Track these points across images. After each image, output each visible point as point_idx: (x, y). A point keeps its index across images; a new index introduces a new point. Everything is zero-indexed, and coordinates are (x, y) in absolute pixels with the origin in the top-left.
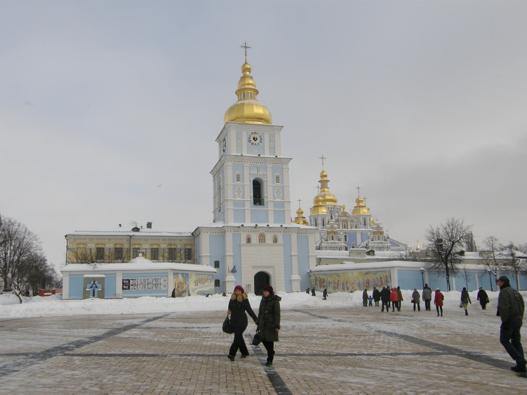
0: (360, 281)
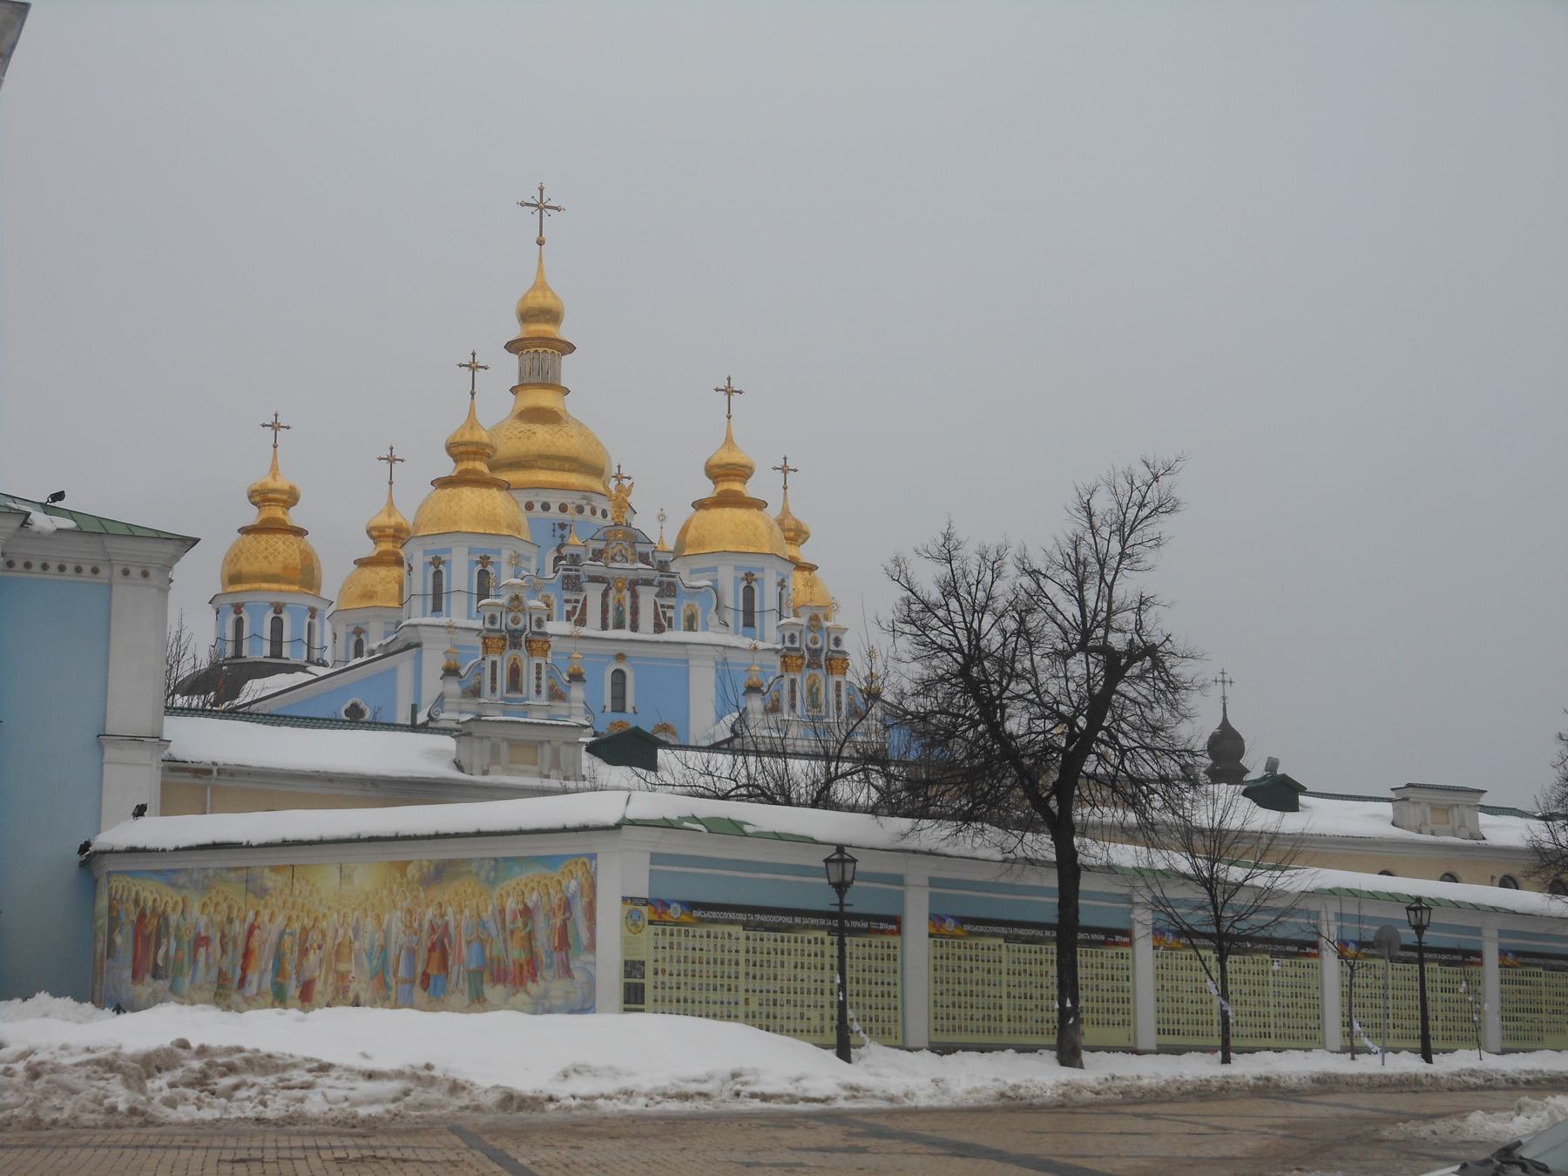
0: (387, 933)
